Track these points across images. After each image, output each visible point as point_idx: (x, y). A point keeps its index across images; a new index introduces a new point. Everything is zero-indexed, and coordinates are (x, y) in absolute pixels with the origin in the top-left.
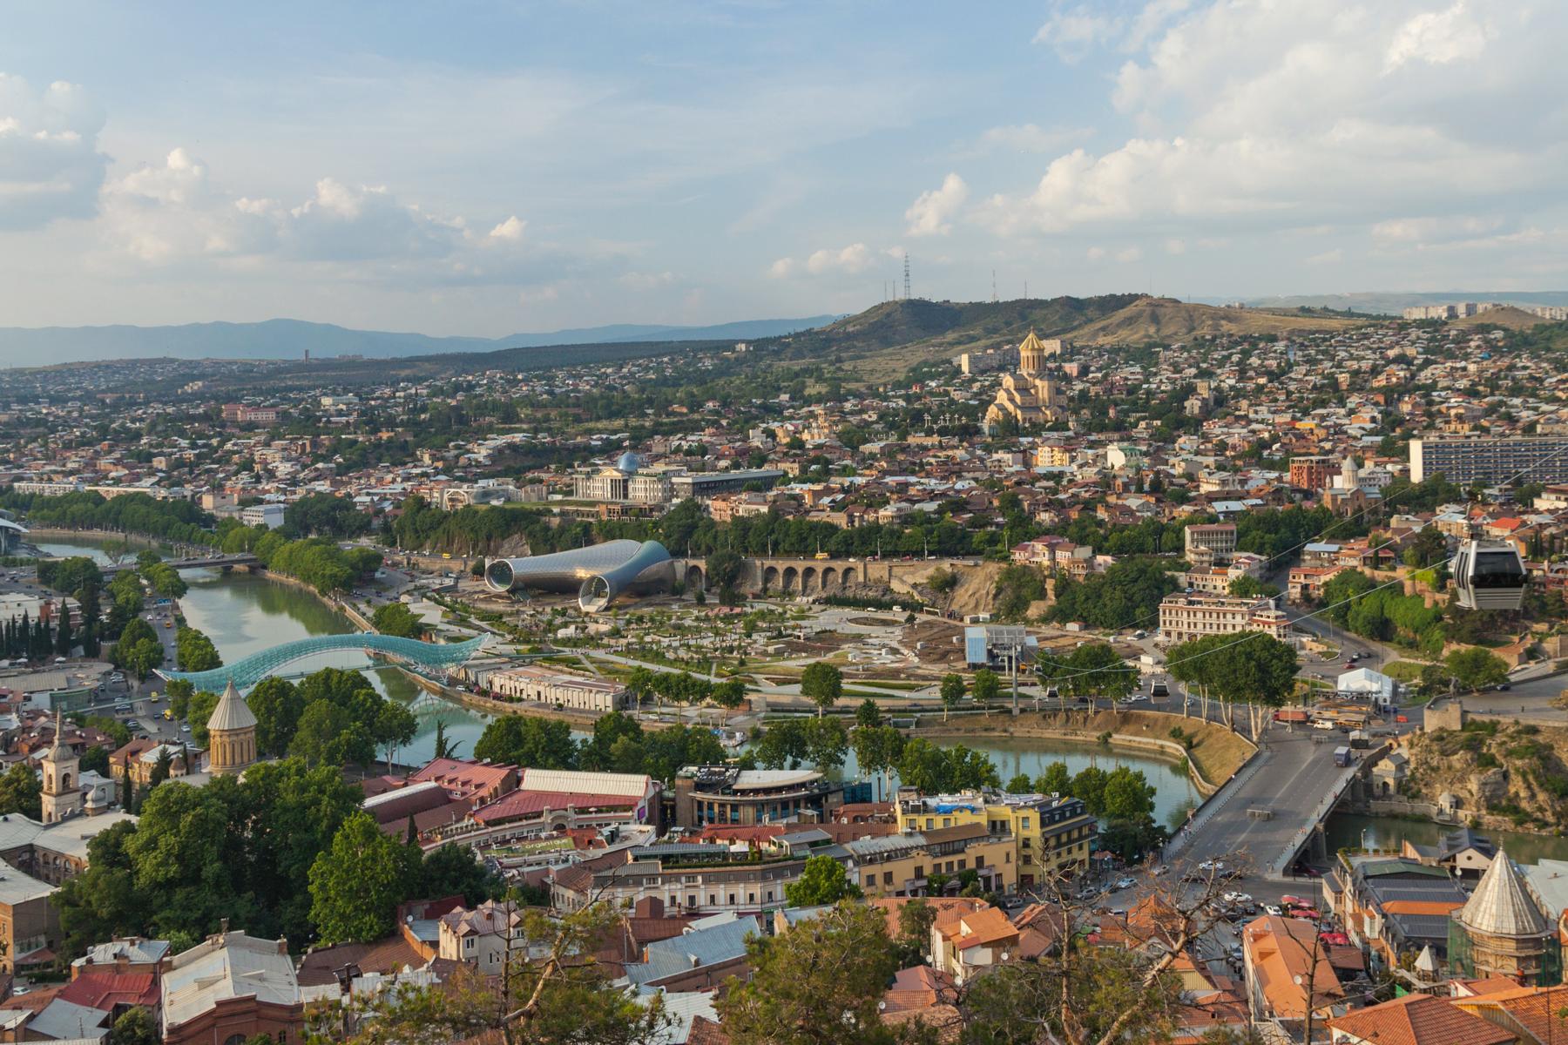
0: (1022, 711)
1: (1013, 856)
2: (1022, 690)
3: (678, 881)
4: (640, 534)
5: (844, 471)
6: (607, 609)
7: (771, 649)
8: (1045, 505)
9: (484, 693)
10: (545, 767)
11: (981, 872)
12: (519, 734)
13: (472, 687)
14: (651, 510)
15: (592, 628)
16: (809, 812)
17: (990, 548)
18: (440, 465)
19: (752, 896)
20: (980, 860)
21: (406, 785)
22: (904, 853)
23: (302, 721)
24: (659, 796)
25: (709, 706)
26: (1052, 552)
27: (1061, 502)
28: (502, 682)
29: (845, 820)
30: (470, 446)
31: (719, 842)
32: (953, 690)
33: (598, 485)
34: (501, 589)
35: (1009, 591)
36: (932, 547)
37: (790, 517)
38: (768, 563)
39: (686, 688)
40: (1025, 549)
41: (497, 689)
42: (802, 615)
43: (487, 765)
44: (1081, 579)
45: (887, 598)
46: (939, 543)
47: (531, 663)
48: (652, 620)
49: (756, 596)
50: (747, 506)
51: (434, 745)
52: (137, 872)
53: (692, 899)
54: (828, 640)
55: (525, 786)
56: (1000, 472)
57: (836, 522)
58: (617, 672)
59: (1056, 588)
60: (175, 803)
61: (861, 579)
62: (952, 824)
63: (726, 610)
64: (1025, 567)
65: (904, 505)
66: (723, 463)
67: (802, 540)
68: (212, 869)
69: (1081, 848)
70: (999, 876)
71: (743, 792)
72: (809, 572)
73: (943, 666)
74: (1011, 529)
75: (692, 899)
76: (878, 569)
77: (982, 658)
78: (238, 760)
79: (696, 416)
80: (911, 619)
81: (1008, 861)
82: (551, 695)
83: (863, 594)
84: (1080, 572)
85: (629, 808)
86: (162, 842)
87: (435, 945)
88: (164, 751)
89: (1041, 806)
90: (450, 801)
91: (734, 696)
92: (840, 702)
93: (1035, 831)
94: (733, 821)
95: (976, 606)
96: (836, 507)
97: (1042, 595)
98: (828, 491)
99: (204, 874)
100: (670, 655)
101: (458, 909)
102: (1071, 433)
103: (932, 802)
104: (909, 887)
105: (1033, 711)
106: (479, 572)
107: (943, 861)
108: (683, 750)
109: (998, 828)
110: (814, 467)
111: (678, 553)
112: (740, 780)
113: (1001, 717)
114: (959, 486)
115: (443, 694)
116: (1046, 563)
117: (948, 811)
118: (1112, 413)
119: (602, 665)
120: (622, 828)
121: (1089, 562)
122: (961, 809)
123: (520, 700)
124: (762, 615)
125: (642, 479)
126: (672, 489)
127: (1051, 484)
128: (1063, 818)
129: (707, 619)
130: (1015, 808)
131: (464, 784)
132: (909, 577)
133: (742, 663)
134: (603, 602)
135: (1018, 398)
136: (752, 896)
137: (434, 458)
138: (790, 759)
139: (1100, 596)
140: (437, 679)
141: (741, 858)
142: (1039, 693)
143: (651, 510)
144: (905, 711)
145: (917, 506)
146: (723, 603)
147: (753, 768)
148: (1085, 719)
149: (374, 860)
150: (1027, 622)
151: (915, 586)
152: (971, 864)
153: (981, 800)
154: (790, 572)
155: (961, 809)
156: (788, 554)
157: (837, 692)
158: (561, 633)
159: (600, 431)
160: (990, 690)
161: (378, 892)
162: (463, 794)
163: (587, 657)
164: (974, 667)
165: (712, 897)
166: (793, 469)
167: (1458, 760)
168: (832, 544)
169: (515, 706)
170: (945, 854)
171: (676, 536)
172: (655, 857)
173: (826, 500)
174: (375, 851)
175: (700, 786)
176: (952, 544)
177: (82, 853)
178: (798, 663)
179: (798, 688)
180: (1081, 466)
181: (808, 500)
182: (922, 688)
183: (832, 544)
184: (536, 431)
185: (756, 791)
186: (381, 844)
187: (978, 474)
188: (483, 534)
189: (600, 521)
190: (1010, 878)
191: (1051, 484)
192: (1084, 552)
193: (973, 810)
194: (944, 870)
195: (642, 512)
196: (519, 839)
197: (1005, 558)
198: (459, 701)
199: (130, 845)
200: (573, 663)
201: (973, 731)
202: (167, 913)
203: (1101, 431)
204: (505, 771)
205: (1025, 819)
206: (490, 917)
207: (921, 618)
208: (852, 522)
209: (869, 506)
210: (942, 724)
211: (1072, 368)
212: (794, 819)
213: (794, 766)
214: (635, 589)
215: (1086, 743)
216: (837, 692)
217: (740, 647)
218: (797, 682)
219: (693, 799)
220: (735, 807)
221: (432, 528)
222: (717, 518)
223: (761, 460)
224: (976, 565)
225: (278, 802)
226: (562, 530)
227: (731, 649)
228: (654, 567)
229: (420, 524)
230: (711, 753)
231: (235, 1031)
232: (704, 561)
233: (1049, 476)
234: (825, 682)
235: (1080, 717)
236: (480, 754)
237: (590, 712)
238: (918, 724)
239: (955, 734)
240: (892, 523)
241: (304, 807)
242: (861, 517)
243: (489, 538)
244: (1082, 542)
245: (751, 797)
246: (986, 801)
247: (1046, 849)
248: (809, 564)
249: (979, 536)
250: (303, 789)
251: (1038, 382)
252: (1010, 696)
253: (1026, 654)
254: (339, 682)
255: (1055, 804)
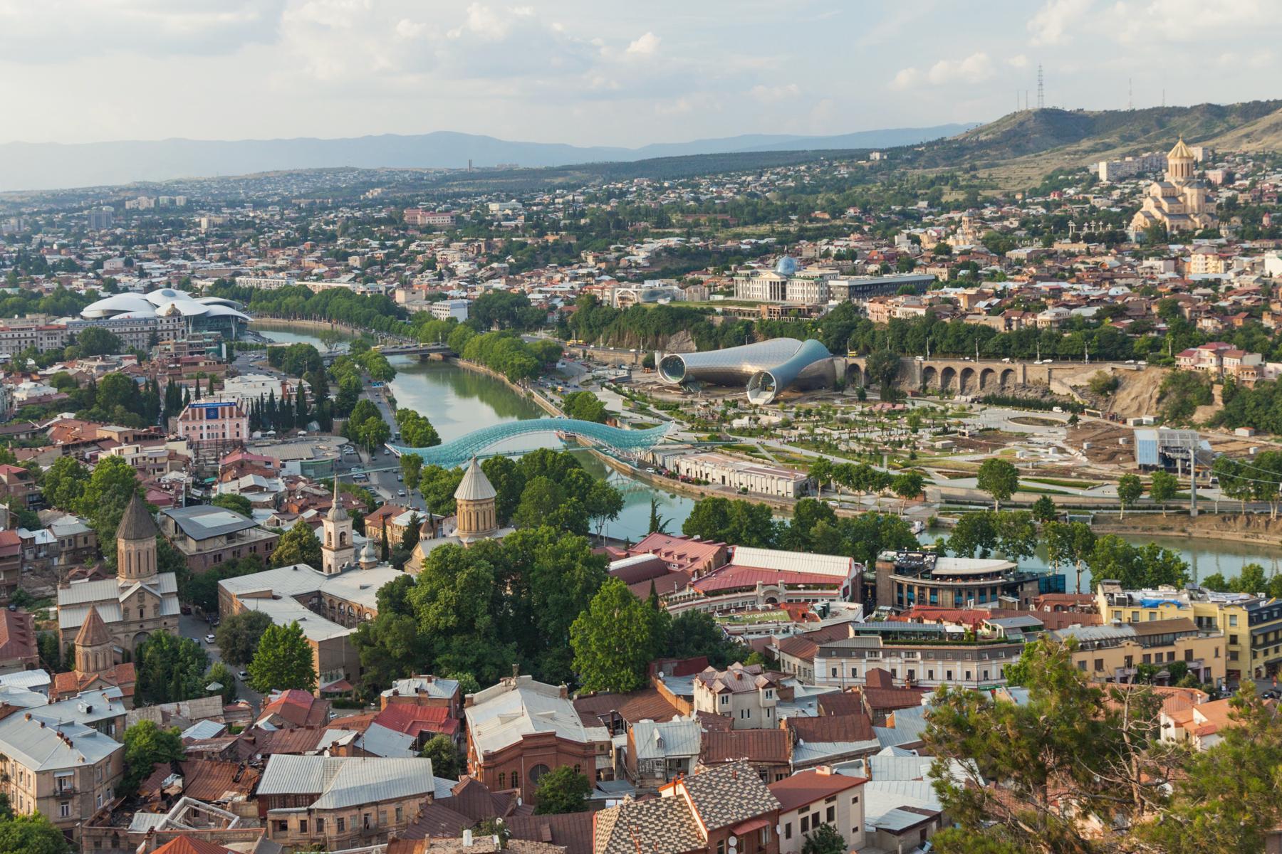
0: (1201, 512)
1: (1222, 652)
2: (1200, 492)
3: (899, 655)
4: (800, 333)
5: (993, 276)
6: (774, 402)
7: (938, 445)
8: (1207, 312)
9: (674, 476)
10: (749, 545)
11: (1191, 665)
12: (725, 514)
13: (660, 470)
14: (810, 311)
15: (764, 420)
16: (1010, 599)
17: (1154, 353)
18: (603, 265)
19: (968, 674)
20: (1189, 654)
21: (628, 556)
22: (1115, 642)
23: (525, 495)
24: (860, 576)
25: (885, 496)
26: (1220, 358)
27: (1224, 309)
28: (688, 465)
29: (1048, 609)
30: (629, 249)
31: (926, 622)
32: (1131, 490)
33: (757, 287)
34: (674, 381)
35: (1174, 396)
36: (1093, 351)
37: (947, 320)
39: (866, 479)
40: (1190, 355)
41: (683, 472)
42: (963, 413)
43: (697, 541)
44: (1251, 386)
45: (1047, 399)
46: (1099, 347)
47: (713, 450)
48: (819, 414)
49: (914, 394)
50: (904, 309)
51: (649, 521)
52: (418, 620)
53: (911, 673)
54: (990, 438)
55: (735, 561)
56: (1153, 279)
57: (993, 325)
58: (793, 460)
59: (1224, 394)
60: (452, 562)
61: (1020, 380)
62: (1158, 618)
63: (888, 406)
64: (1191, 372)
65: (1062, 310)
66: (873, 268)
67: (959, 341)
68: (483, 621)
70: (1208, 669)
71: (942, 577)
72: (968, 372)
73: (1113, 466)
74: (1174, 335)
75: (911, 673)
76: (1038, 370)
77: (1154, 460)
78: (481, 527)
79: (838, 222)
80: (1074, 420)
81: (1217, 656)
82: (736, 480)
83: (1021, 395)
84: (1250, 380)
85: (835, 587)
86: (441, 595)
87: (690, 699)
88: (414, 517)
89: (1248, 605)
90: (669, 572)
91: (912, 487)
92: (1017, 497)
93: (1242, 628)
94: (932, 603)
95: (1139, 409)
96: (991, 310)
97: (1209, 400)
98: (982, 295)
99: (477, 625)
100: (843, 447)
101: (710, 669)
102: (1223, 241)
103: (1137, 595)
104: (1119, 675)
105: (1212, 513)
106: (649, 364)
107: (1153, 652)
108: (876, 535)
109: (1205, 624)
110: (962, 272)
111: (838, 351)
112: (938, 566)
113: (1179, 518)
114: (1113, 292)
115: (634, 475)
116: (1213, 368)
117: (1155, 605)
118: (1266, 220)
119: (779, 454)
120: (832, 604)
121: (1259, 369)
122: (1168, 603)
123: (707, 483)
124: (924, 412)
125: (800, 281)
126: (829, 292)
127: (1209, 291)
128: (1271, 618)
129: (871, 414)
130: (1222, 605)
131: (680, 557)
132: (1069, 380)
133: (913, 457)
134: (769, 396)
135: (1165, 206)
136: (968, 674)
137: (597, 260)
138: (979, 548)
139: (1271, 403)
140: (628, 461)
141: (957, 639)
142: (1217, 494)
143: (810, 311)
144: (1080, 508)
145: (1074, 312)
146: (884, 399)
147: (944, 555)
148: (1267, 523)
149: (630, 621)
150: (1193, 425)
151: (1075, 388)
152: (1180, 657)
153: (1186, 596)
154: (949, 372)
155: (1168, 603)
156: (945, 355)
157: (1014, 488)
158: (737, 423)
159: (748, 236)
160: (1169, 491)
161: (634, 649)
162: (680, 566)
163: (764, 446)
164: (1146, 468)
165: (931, 673)
166: (944, 274)
168: (990, 346)
169: (702, 488)
170: (1154, 645)
171: (835, 335)
172: (874, 632)
173: (982, 304)
174: (630, 613)
175: (899, 570)
176: (1112, 349)
177: (370, 602)
178: (966, 459)
179: (974, 482)
180: (1238, 274)
181: (963, 304)
182: (1094, 487)
183: (990, 346)
184: (689, 235)
185: (955, 577)
186: (636, 607)
187: (1130, 281)
188: (652, 329)
189: (762, 320)
190: (1218, 671)
191: (1209, 291)
192: (1254, 359)
193: (1179, 605)
194: (1153, 661)
195: (800, 312)
196: (738, 610)
198: (650, 482)
199: (414, 596)
200: (751, 451)
201: (1150, 529)
202: (447, 657)
203: (1255, 239)
204: (715, 548)
205: (1233, 617)
206: (740, 677)
207: (1084, 419)
208: (1010, 326)
209: (1027, 310)
210: (1119, 522)
211: (1216, 175)
212: (996, 605)
213: (984, 555)
214: (799, 384)
215: (1268, 546)
216: (1014, 488)
217: (908, 441)
218: (974, 476)
219: (893, 581)
220: (934, 591)
221: (605, 323)
222: (874, 319)
223: (910, 265)
224: (1138, 370)
225: (536, 566)
226: (725, 328)
227: (900, 444)
228: (815, 365)
229: (594, 320)
230: (904, 541)
231: (538, 762)
232: (862, 359)
233: (1206, 283)
234: (1002, 477)
235: (1262, 521)
236: (690, 530)
237: (772, 496)
238: (1094, 520)
239: (1132, 532)
240: (1050, 328)
241: (559, 572)
242: (1019, 321)
243: (657, 334)
244: (1249, 348)
245: (950, 583)
246: (1192, 598)
247: (1254, 644)
248: (968, 365)
249: (1140, 341)
250: (557, 555)
251: (1186, 190)
252: (1188, 497)
253: (1202, 456)
254: (554, 462)
255: (1262, 604)
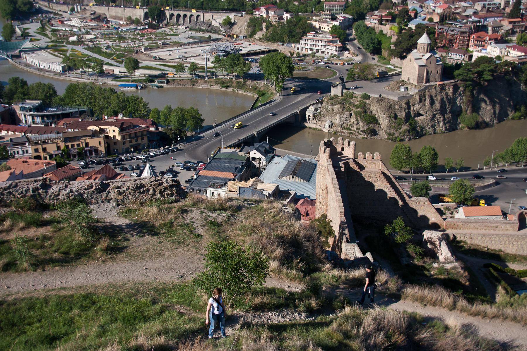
11: (86, 149)
38: (171, 12)
61: (202, 20)
69: (143, 139)
97: (261, 29)
107: (70, 144)
116: (265, 16)
154: (179, 16)
167: (336, 107)
197: (252, 14)
